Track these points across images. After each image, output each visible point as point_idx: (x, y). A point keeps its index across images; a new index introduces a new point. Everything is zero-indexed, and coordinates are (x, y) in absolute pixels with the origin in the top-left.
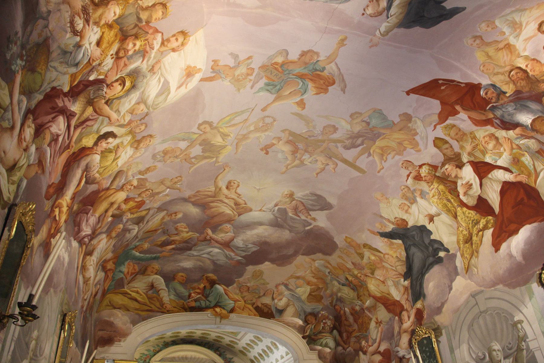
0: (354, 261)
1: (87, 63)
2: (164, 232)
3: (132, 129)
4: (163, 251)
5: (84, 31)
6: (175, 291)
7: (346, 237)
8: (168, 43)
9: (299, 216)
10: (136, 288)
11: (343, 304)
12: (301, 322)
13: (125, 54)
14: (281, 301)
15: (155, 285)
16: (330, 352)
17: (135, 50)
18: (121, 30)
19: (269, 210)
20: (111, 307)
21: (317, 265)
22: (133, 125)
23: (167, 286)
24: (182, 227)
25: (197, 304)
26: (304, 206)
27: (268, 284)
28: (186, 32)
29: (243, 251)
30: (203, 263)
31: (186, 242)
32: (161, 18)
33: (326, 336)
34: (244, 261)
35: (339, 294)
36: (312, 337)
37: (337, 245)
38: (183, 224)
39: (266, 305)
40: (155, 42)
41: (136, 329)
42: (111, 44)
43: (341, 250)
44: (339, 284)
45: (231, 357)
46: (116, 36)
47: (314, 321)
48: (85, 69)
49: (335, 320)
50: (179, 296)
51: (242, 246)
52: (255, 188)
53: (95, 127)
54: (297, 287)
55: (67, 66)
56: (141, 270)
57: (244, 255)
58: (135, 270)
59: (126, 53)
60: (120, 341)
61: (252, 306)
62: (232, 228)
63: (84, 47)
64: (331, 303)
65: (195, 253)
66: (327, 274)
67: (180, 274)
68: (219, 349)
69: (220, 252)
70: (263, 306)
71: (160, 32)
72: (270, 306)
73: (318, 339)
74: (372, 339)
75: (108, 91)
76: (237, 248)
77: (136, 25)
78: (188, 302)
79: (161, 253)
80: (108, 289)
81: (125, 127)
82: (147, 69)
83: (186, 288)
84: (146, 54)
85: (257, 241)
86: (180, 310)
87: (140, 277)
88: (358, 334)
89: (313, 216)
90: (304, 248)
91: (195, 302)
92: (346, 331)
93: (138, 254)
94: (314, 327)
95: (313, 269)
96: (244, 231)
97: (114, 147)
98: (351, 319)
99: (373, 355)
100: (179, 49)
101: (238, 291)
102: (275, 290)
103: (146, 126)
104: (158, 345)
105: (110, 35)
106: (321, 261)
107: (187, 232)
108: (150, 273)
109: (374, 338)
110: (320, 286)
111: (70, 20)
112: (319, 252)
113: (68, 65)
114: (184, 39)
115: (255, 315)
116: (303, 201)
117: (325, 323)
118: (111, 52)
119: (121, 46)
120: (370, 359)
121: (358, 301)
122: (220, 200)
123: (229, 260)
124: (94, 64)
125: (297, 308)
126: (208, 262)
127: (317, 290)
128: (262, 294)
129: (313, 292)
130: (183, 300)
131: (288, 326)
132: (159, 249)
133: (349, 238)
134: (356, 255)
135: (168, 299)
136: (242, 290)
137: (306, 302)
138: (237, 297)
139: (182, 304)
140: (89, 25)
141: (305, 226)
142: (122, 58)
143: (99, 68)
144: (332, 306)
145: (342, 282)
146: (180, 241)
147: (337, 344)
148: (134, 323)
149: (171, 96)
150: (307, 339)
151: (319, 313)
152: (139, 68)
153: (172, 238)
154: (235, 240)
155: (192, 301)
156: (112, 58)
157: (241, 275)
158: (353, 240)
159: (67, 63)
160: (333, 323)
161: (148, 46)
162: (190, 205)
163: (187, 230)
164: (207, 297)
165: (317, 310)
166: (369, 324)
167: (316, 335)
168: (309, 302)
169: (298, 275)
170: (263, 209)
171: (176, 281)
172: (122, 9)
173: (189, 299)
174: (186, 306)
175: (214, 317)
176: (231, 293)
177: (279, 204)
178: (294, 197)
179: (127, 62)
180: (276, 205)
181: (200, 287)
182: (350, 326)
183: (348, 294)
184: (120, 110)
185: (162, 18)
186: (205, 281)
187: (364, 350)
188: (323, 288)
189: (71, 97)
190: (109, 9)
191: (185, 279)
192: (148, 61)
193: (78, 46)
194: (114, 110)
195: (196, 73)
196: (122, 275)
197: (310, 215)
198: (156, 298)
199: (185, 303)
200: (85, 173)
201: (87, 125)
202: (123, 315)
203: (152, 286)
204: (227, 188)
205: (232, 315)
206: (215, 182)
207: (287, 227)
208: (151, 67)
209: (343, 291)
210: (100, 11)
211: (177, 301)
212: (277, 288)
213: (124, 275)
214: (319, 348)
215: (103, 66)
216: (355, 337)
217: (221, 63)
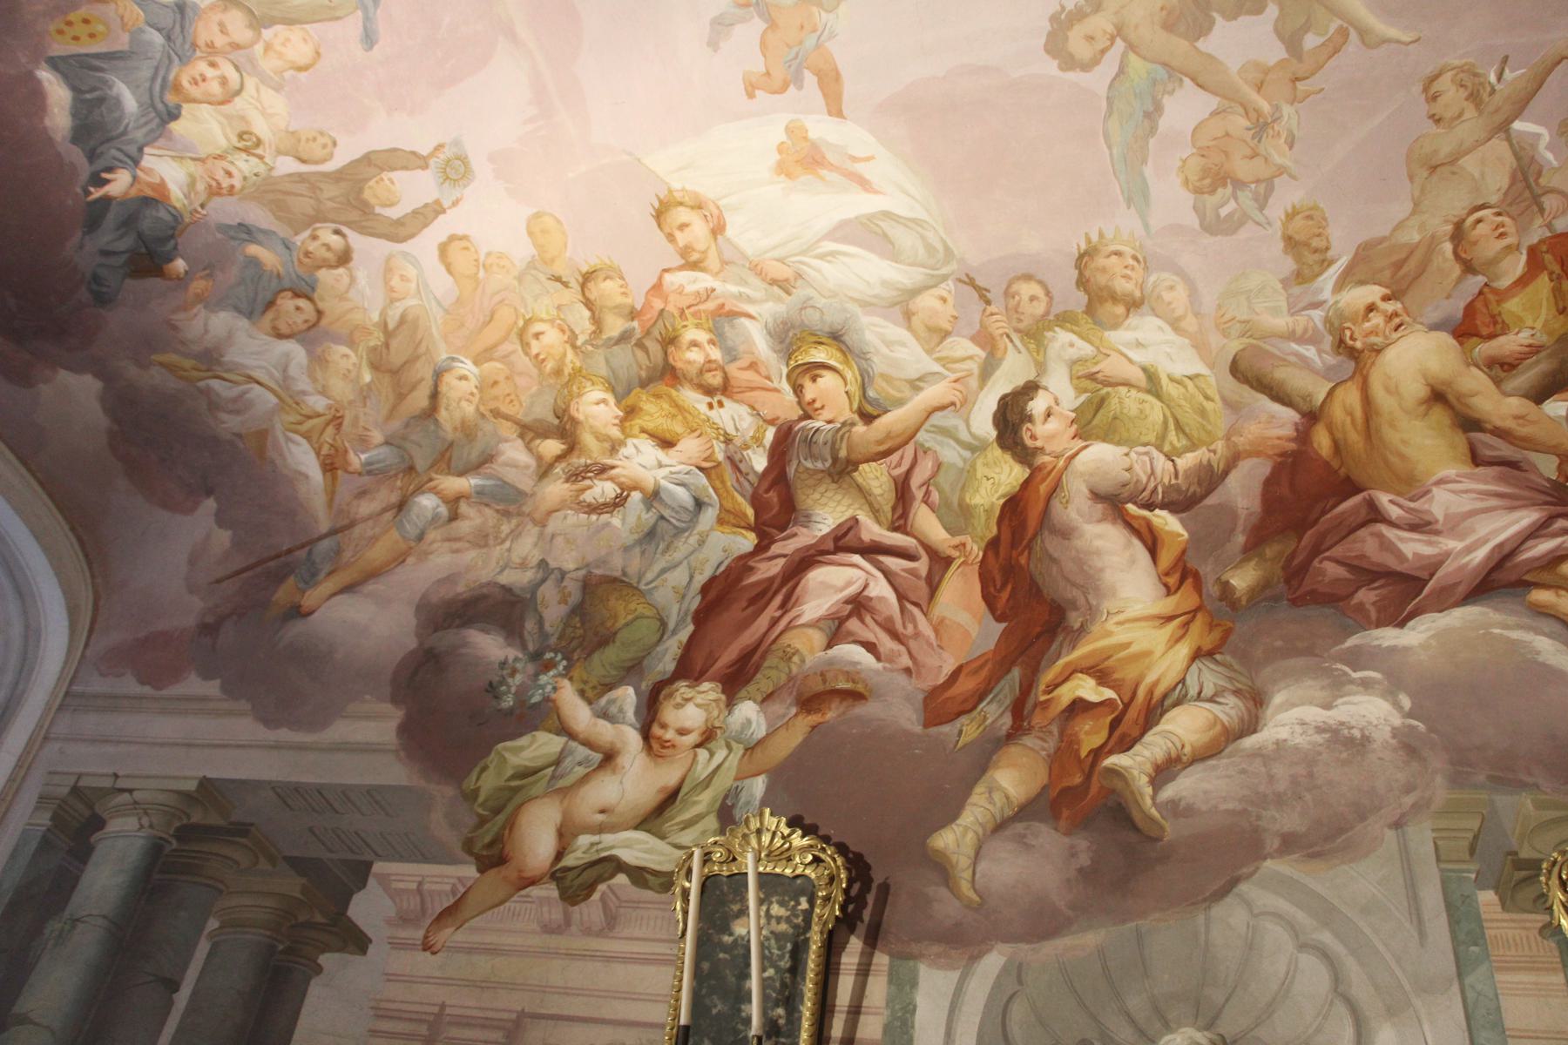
1: (708, 477)
3: (1017, 331)
5: (622, 479)
8: (694, 250)
13: (716, 370)
17: (711, 342)
18: (644, 384)
22: (998, 325)
28: (657, 205)
32: (621, 282)
40: (690, 288)
42: (680, 408)
46: (658, 396)
48: (723, 482)
53: (951, 454)
55: (686, 534)
59: (714, 366)
63: (664, 483)
71: (660, 278)
75: (826, 414)
77: (640, 345)
81: (999, 354)
82: (779, 300)
84: (727, 308)
97: (1080, 391)
100: (715, 212)
103: (1028, 277)
105: (654, 413)
111: (585, 513)
113: (685, 530)
114: (681, 204)
118: (703, 408)
119: (691, 381)
124: (720, 456)
140: (613, 467)
142: (726, 378)
143: (738, 442)
149: (901, 206)
152: (770, 325)
156: (721, 404)
159: (679, 532)
161: (701, 307)
172: (593, 384)
179: (744, 363)
184: (915, 376)
185: (622, 278)
189: (783, 528)
190: (586, 417)
192: (750, 300)
193: (653, 497)
194: (907, 392)
195: (805, 138)
200: (1131, 507)
201: (927, 483)
208: (775, 288)
210: (588, 439)
215: (737, 430)
217: (758, 65)
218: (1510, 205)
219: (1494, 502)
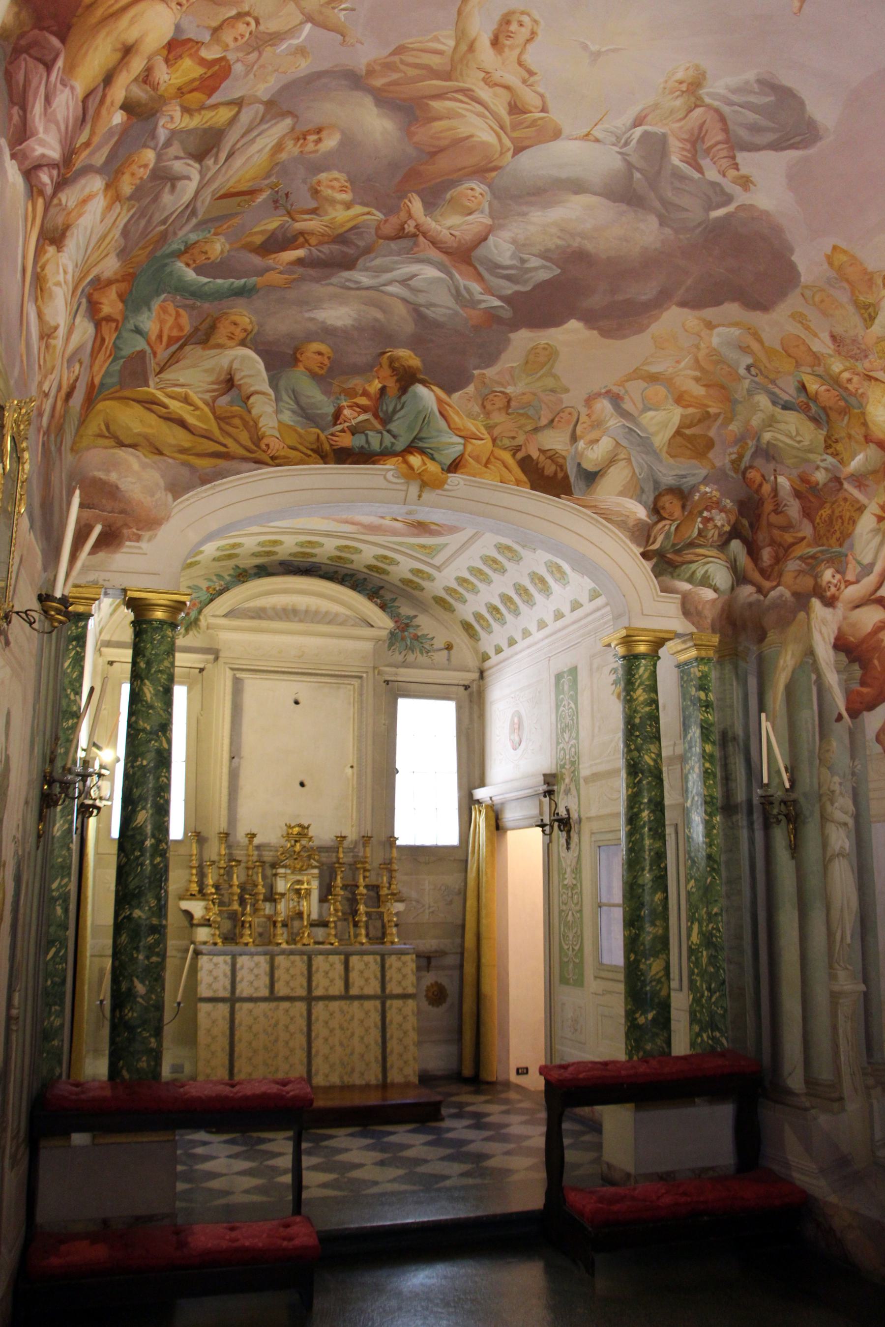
0: (839, 330)
2: (276, 202)
4: (268, 269)
6: (297, 402)
7: (835, 248)
9: (700, 169)
10: (182, 385)
11: (772, 466)
12: (641, 513)
14: (595, 447)
15: (237, 377)
16: (714, 601)
19: (613, 139)
20: (112, 442)
21: (715, 341)
23: (274, 383)
24: (332, 188)
25: (357, 442)
26: (726, 130)
27: (567, 390)
29: (508, 278)
30: (384, 311)
31: (341, 239)
33: (706, 556)
34: (507, 313)
35: (767, 436)
36: (668, 556)
37: (798, 275)
38: (335, 174)
39: (552, 456)
41: (182, 506)
43: (808, 293)
44: (774, 403)
45: (412, 613)
47: (677, 513)
49: (741, 513)
50: (306, 414)
51: (508, 262)
52: (585, 47)
54: (647, 409)
56: (197, 329)
57: (510, 292)
58: (181, 329)
60: (138, 538)
61: (514, 455)
62: (488, 197)
64: (735, 463)
65: (364, 279)
66: (742, 371)
67: (316, 346)
68: (382, 592)
69: (439, 280)
70: (542, 458)
72: (564, 458)
73: (683, 563)
74: (859, 563)
76: (494, 267)
78: (332, 435)
79: (262, 275)
80: (102, 385)
83: (327, 393)
85: (557, 247)
86: (309, 456)
87: (193, 352)
88: (812, 551)
89: (744, 171)
90: (689, 282)
91: (353, 434)
92: (773, 543)
93: (190, 275)
94: (677, 528)
95: (701, 355)
96: (525, 209)
98: (794, 509)
99: (857, 607)
101: (477, 409)
102: (584, 411)
104: (219, 576)
106: (732, 330)
107: (348, 206)
108: (222, 340)
109: (867, 560)
110: (712, 410)
112: (734, 300)
115: (518, 483)
116: (726, 110)
117: (707, 520)
120: (845, 618)
121: (825, 456)
122: (464, 91)
123: (464, 306)
125: (637, 471)
126: (401, 310)
128: (544, 421)
129: (689, 427)
130: (317, 427)
131: (604, 518)
132: (256, 260)
133: (845, 252)
134: (851, 309)
135: (276, 425)
136: (489, 407)
137: (664, 455)
138: (472, 426)
139: (313, 438)
141: (711, 206)
144: (736, 470)
145: (786, 397)
146: (323, 235)
147: (740, 578)
148: (177, 489)
150: (655, 560)
151: (694, 488)
153: (299, 226)
154: (491, 238)
155: (343, 431)
157: (490, 359)
158: (854, 260)
160: (732, 522)
162: (368, 101)
163: (346, 197)
164: (386, 421)
165: (691, 481)
166: (854, 522)
167: (678, 552)
168: (672, 456)
169: (654, 369)
170: (597, 133)
171: (301, 368)
173: (335, 424)
174: (327, 447)
175: (403, 481)
176: (458, 413)
177: (649, 118)
178: (702, 92)
180: (638, 122)
181: (368, 388)
182: (788, 527)
183: (798, 434)
186: (386, 371)
187: (828, 594)
188: (718, 415)
191: (327, 362)
196: (141, 344)
197: (736, 167)
198: (242, 418)
199: (322, 437)
202: (144, 466)
203: (229, 383)
204: (495, 42)
205: (454, 479)
206: (460, 12)
207: (657, 204)
209: (782, 426)
211: (299, 429)
213: (149, 344)
214: (686, 586)
216: (800, 558)
218: (256, 37)
219: (63, 128)
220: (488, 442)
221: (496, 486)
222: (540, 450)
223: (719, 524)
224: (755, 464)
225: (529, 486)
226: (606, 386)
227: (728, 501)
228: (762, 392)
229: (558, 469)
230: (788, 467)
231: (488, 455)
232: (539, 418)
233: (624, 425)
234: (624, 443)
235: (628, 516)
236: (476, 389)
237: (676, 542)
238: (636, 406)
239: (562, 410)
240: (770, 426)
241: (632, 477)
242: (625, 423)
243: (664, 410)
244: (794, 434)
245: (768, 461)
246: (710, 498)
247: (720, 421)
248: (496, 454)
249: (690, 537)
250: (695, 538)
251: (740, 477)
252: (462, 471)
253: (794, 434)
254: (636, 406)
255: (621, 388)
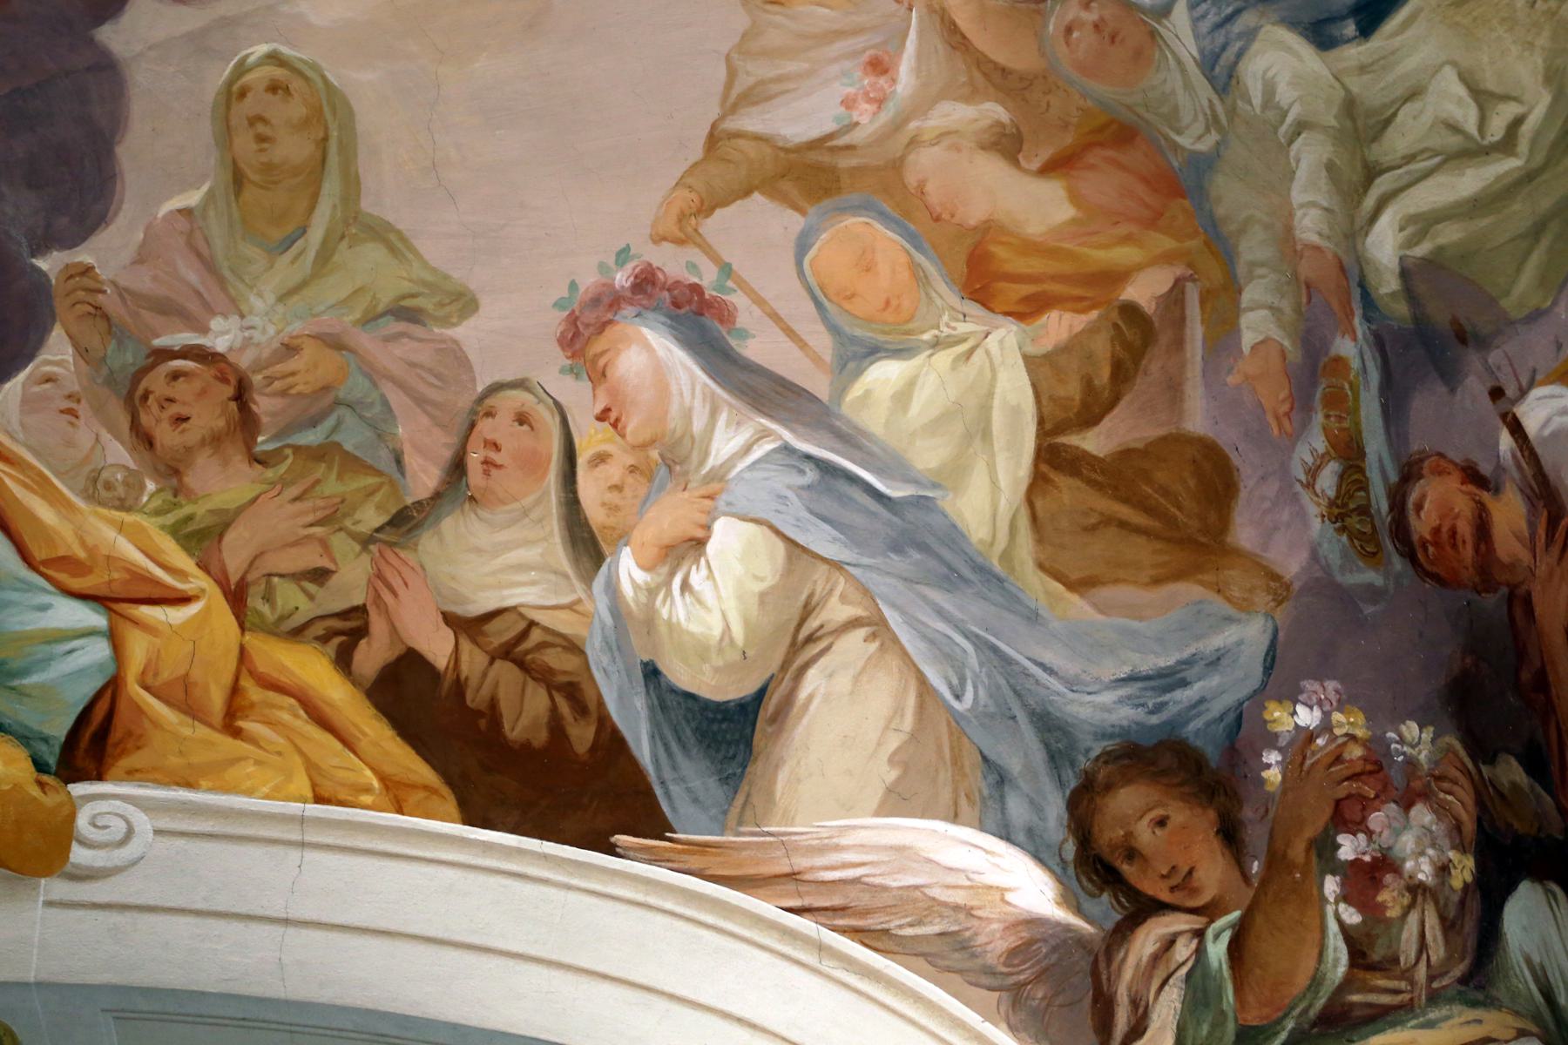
11: (1474, 387)
27: (464, 303)
47: (1213, 872)
49: (1481, 748)
61: (343, 661)
70: (473, 661)
72: (574, 647)
101: (118, 454)
102: (579, 398)
110: (1145, 290)
115: (397, 796)
127: (1122, 374)
128: (424, 478)
129: (1090, 415)
136: (166, 436)
137: (1036, 586)
144: (1366, 547)
160: (1469, 827)
183: (1482, 97)
188: (1174, 298)
212: (598, 376)
220: (212, 601)
221: (302, 820)
222: (450, 619)
223: (1424, 872)
224: (1415, 447)
225: (451, 805)
226: (623, 255)
227: (1411, 729)
228: (1248, 19)
229: (564, 708)
230: (1536, 315)
231: (227, 679)
232: (399, 461)
233: (787, 449)
234: (822, 540)
235: (968, 911)
236: (82, 351)
237: (1253, 1018)
238: (802, 344)
239: (482, 407)
240: (1372, 172)
241: (921, 707)
242: (788, 436)
243: (937, 344)
244: (1468, 117)
245: (1450, 376)
246: (1338, 759)
247: (1196, 331)
248: (262, 667)
249: (1316, 981)
250: (1347, 984)
251: (1398, 564)
252: (125, 763)
253: (1468, 117)
254: (802, 344)
255: (693, 254)
